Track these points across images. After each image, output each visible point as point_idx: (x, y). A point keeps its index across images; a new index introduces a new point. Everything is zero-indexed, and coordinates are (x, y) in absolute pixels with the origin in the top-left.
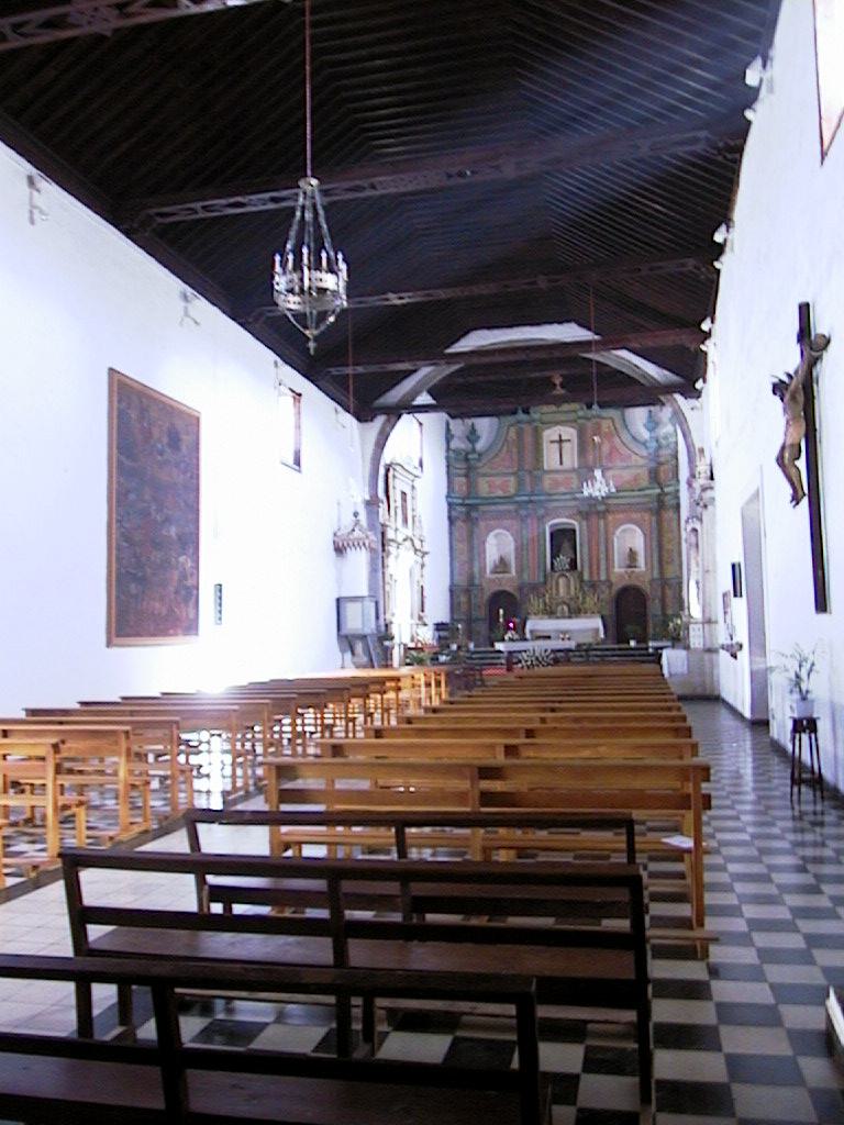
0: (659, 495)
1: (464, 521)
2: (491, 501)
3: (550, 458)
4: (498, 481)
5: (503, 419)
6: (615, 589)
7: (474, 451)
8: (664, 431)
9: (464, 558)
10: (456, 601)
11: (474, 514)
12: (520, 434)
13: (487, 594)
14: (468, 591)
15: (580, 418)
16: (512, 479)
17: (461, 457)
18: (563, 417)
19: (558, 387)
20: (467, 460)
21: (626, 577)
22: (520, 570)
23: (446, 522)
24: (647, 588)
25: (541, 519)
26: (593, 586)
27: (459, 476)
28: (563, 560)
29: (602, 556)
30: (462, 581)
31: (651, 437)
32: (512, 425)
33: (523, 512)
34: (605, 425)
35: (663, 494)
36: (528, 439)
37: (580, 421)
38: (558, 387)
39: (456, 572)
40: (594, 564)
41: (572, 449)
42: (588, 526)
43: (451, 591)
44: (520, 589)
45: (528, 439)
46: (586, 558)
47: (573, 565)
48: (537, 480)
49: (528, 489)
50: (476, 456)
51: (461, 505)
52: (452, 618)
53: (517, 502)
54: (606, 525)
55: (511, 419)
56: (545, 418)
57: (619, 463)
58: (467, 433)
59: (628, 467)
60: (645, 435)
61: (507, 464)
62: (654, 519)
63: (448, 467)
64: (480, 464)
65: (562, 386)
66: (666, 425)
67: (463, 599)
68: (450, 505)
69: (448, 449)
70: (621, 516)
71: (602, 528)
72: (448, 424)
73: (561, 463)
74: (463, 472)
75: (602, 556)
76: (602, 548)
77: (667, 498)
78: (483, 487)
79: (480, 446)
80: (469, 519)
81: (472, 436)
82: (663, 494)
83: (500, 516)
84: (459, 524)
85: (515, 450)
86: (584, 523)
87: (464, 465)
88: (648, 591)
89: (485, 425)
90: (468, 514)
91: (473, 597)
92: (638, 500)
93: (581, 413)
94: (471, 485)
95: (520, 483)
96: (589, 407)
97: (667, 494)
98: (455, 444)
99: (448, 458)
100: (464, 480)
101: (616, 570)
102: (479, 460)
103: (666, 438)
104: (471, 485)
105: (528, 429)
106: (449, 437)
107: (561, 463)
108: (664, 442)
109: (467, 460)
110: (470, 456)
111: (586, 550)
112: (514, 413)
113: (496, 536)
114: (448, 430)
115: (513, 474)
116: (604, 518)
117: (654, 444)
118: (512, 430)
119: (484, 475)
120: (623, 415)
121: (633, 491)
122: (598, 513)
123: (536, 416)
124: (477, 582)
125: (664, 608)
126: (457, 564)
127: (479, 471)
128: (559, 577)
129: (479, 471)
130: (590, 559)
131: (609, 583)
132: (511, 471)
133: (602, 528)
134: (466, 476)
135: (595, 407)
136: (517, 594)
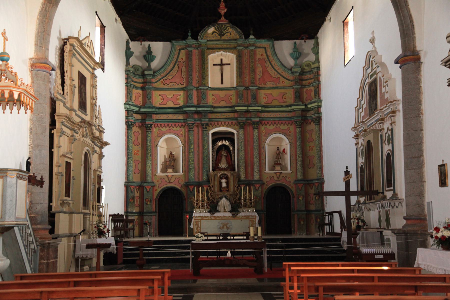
0: (303, 110)
1: (140, 127)
2: (162, 110)
3: (213, 79)
4: (169, 94)
5: (174, 43)
6: (266, 188)
7: (149, 68)
8: (306, 59)
9: (139, 158)
10: (131, 195)
11: (148, 122)
12: (189, 56)
13: (158, 190)
14: (141, 187)
15: (240, 46)
16: (182, 93)
17: (139, 73)
18: (225, 45)
19: (223, 18)
20: (143, 75)
21: (276, 178)
22: (187, 170)
23: (124, 127)
24: (292, 188)
25: (205, 127)
26: (249, 183)
27: (137, 88)
28: (223, 165)
29: (256, 160)
30: (136, 179)
31: (296, 65)
32: (183, 49)
33: (190, 121)
34: (260, 52)
35: (306, 110)
36: (195, 61)
37: (238, 48)
38: (223, 18)
39: (132, 169)
40: (248, 165)
41: (232, 71)
42: (245, 135)
43: (127, 187)
44: (186, 185)
45: (195, 61)
46: (242, 161)
47: (231, 167)
48: (202, 96)
49: (195, 102)
50: (151, 72)
51: (137, 113)
52: (127, 212)
53: (186, 113)
54: (259, 133)
55: (182, 44)
56: (211, 44)
57: (269, 84)
58: (145, 53)
59: (276, 88)
60: (291, 62)
61: (178, 80)
62: (298, 130)
63: (127, 79)
64: (154, 80)
65: (226, 16)
66: (307, 55)
67: (137, 194)
68: (128, 111)
69: (128, 63)
70: (272, 127)
71: (256, 138)
72: (128, 43)
73: (222, 83)
74: (140, 85)
75: (256, 160)
76: (256, 153)
77: (309, 114)
78: (157, 99)
79: (155, 64)
80: (145, 128)
81: (148, 56)
82: (306, 110)
83: (169, 124)
84: (135, 129)
85: (184, 69)
86: (241, 132)
87: (141, 81)
88: (293, 190)
89: (159, 48)
90: (143, 121)
91: (145, 192)
92: (284, 115)
93: (240, 42)
94: (146, 97)
95: (188, 97)
96: (247, 37)
97: (310, 110)
98: (133, 61)
99: (127, 71)
100: (140, 92)
101: (267, 171)
102: (154, 75)
103: (308, 65)
104: (146, 97)
105: (195, 52)
106: (129, 54)
107: (222, 83)
108: (307, 69)
109: (143, 75)
110: (146, 72)
111: (242, 154)
112: (184, 38)
113: (167, 140)
114: (128, 48)
115: (182, 89)
116: (258, 128)
117: (299, 70)
118: (183, 52)
119: (157, 89)
120: (273, 45)
121: (282, 106)
122: (254, 123)
123: (203, 42)
124: (149, 179)
125: (307, 203)
126: (132, 164)
127: (155, 85)
128: (221, 178)
129: (155, 85)
130: (246, 162)
131: (261, 182)
132: (181, 86)
133: (256, 138)
134: (143, 88)
135: (252, 37)
136: (184, 191)
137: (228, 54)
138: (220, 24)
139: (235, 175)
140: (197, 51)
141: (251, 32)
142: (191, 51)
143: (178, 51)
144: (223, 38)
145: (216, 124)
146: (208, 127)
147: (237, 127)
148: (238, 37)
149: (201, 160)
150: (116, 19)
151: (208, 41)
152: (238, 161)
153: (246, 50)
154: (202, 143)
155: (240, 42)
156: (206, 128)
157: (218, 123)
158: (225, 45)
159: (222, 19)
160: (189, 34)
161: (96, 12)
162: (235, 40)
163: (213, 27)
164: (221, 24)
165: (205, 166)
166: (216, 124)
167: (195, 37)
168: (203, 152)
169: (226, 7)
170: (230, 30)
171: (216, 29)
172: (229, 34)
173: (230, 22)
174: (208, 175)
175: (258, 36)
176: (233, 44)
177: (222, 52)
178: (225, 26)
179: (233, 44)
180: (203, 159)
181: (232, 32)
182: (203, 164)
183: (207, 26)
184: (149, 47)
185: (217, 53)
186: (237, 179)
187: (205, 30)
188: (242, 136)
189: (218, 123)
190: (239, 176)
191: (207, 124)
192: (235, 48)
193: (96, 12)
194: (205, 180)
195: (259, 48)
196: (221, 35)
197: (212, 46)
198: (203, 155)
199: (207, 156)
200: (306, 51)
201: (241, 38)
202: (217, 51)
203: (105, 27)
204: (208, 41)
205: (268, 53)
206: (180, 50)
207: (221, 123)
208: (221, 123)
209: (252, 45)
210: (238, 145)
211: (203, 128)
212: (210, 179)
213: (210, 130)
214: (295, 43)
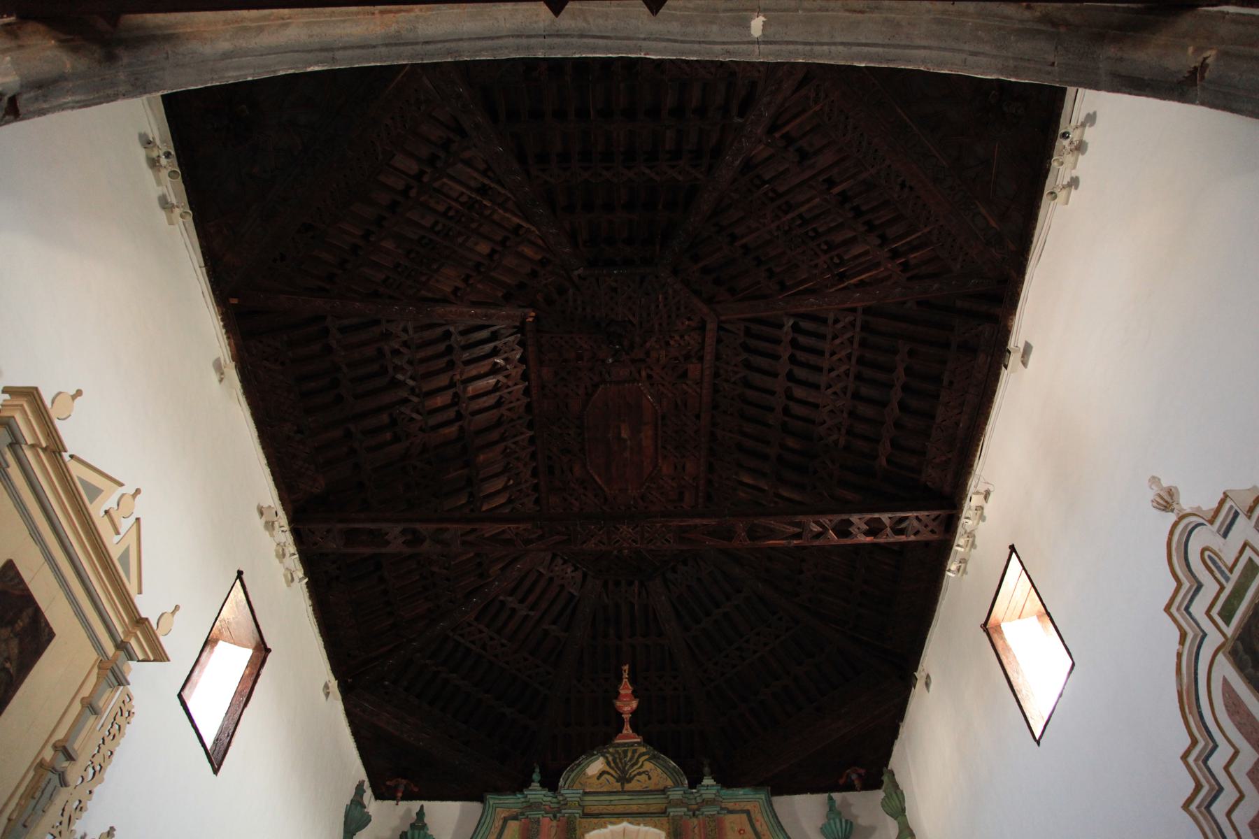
5: (492, 800)
18: (636, 805)
32: (515, 818)
37: (672, 811)
55: (512, 802)
72: (359, 789)
93: (676, 794)
96: (695, 782)
112: (521, 785)
118: (514, 826)
120: (770, 804)
135: (708, 781)
137: (643, 828)
138: (619, 745)
140: (554, 823)
141: (706, 769)
142: (538, 821)
143: (498, 823)
144: (628, 787)
148: (669, 783)
150: (326, 686)
151: (585, 793)
153: (695, 821)
155: (676, 794)
158: (636, 805)
159: (625, 732)
160: (536, 777)
161: (240, 573)
162: (664, 791)
163: (601, 759)
164: (624, 745)
167: (551, 784)
169: (635, 694)
170: (648, 766)
171: (608, 763)
172: (644, 777)
173: (647, 741)
175: (727, 780)
176: (655, 803)
177: (625, 824)
178: (635, 751)
179: (655, 803)
181: (653, 772)
183: (583, 752)
184: (421, 814)
185: (610, 827)
187: (579, 764)
192: (664, 813)
193: (240, 573)
195: (730, 812)
196: (624, 779)
197: (595, 810)
200: (863, 821)
201: (677, 784)
202: (612, 823)
203: (268, 651)
204: (585, 793)
205: (758, 826)
206: (505, 820)
209: (712, 802)
214: (831, 798)
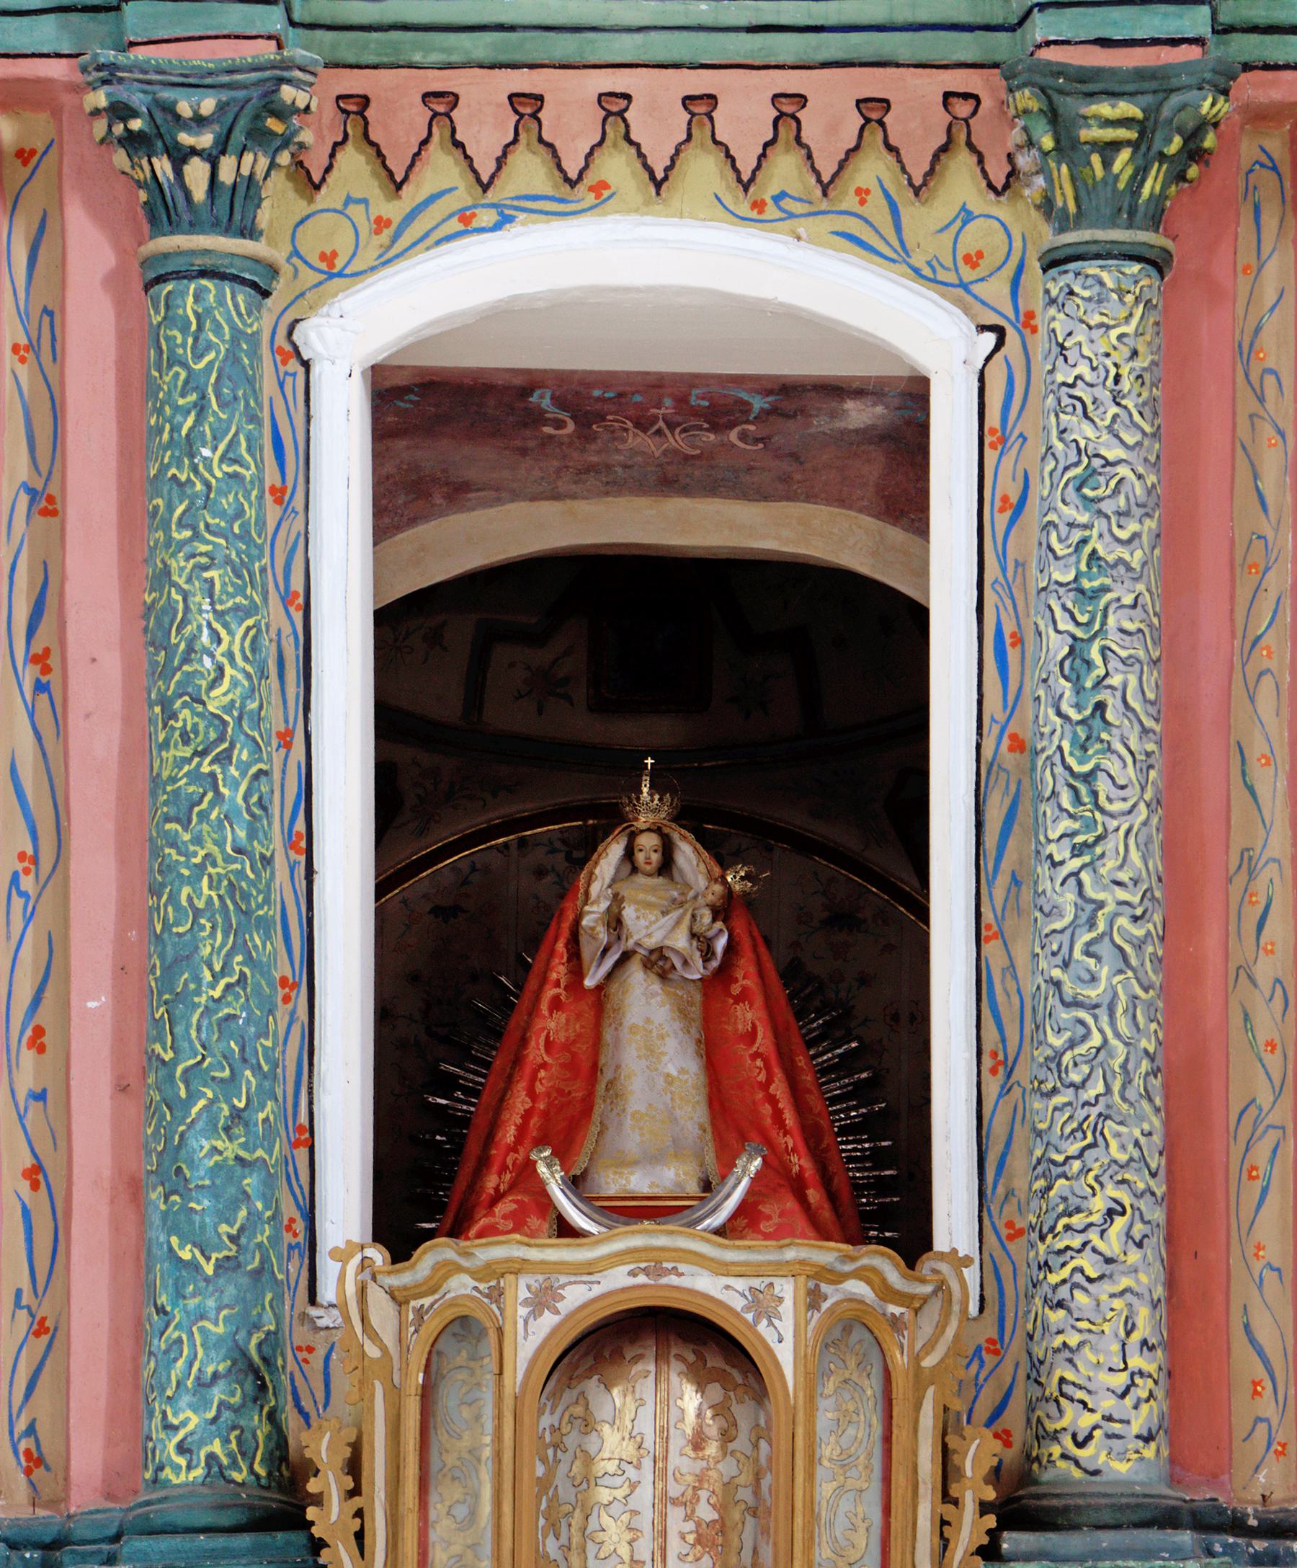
46: (1107, 1024)
86: (1102, 323)
111: (1107, 872)
139: (929, 1344)
145: (484, 127)
146: (278, 203)
147: (1011, 228)
149: (93, 1003)
152: (992, 1060)
154: (146, 574)
156: (235, 208)
157: (527, 106)
165: (207, 1150)
166: (484, 127)
168: (155, 812)
174: (257, 1374)
180: (156, 978)
182: (149, 1084)
186: (977, 1454)
188: (1116, 442)
189: (527, 106)
190: (1011, 1376)
191: (257, 116)
194: (184, 1474)
198: (152, 876)
199: (239, 909)
207: (614, 107)
208: (614, 107)
210: (997, 649)
211: (164, 210)
212: (323, 1448)
213: (334, 272)
